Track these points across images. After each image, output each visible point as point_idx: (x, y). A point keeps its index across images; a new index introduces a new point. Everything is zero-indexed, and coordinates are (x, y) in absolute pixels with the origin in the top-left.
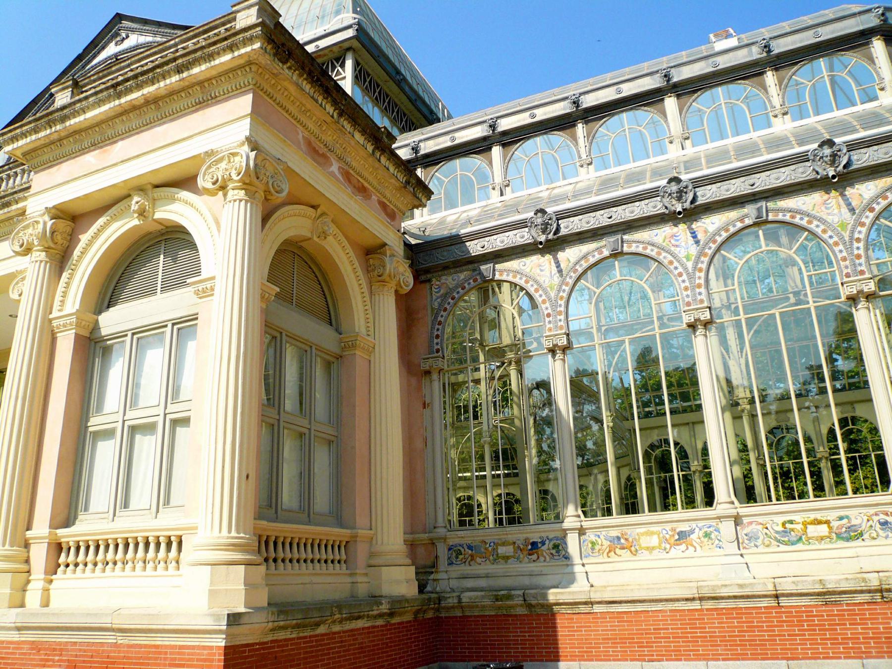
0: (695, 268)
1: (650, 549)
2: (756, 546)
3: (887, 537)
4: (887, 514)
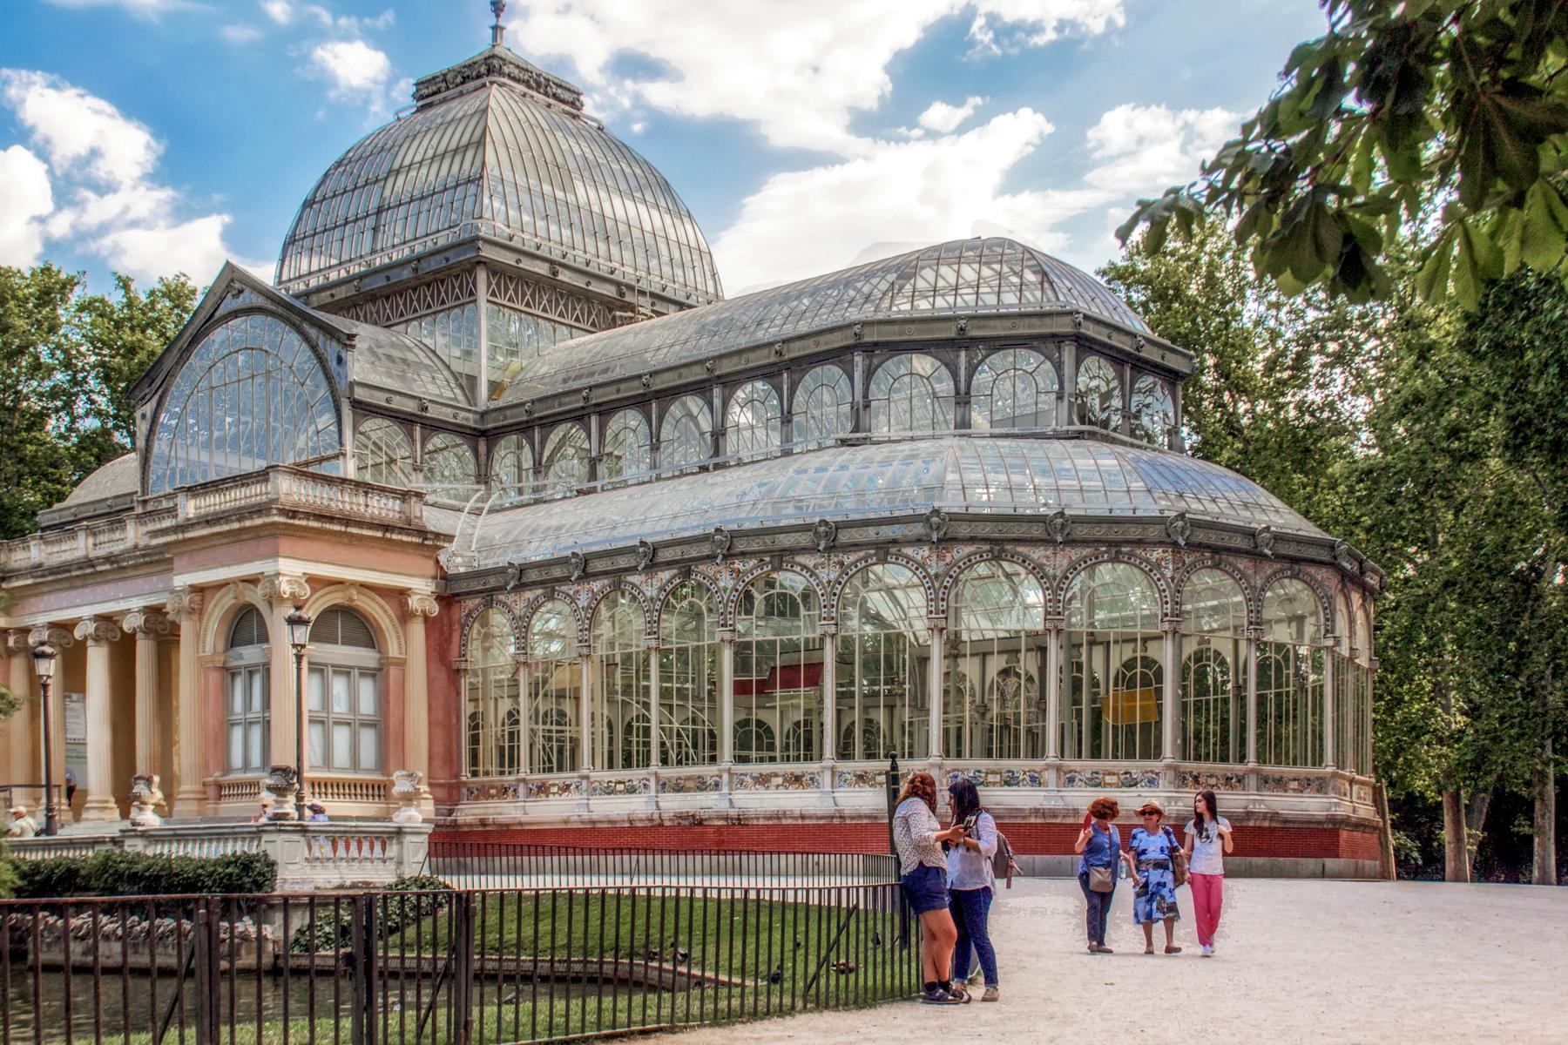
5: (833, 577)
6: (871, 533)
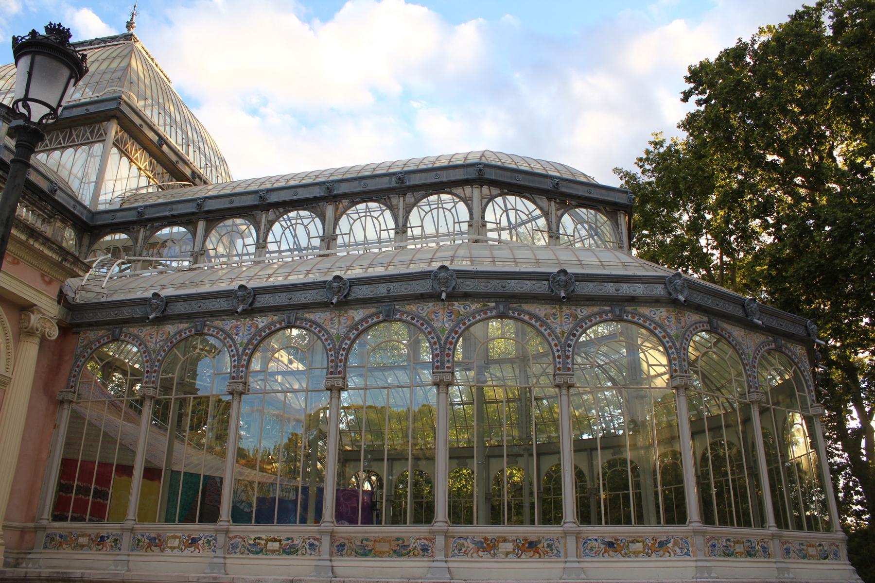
0: (244, 352)
1: (173, 548)
2: (236, 553)
3: (310, 555)
4: (315, 539)
5: (566, 328)
6: (610, 289)
